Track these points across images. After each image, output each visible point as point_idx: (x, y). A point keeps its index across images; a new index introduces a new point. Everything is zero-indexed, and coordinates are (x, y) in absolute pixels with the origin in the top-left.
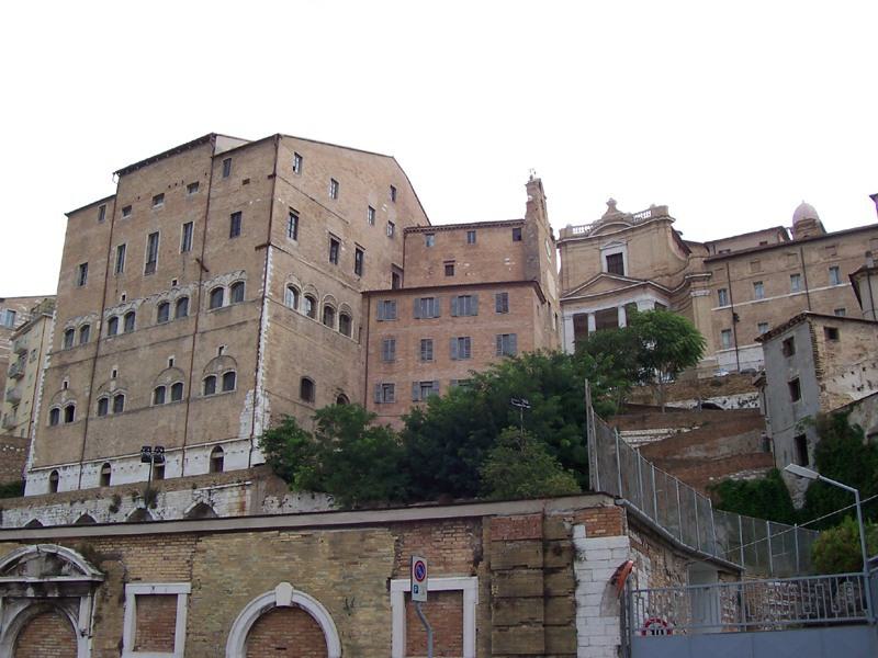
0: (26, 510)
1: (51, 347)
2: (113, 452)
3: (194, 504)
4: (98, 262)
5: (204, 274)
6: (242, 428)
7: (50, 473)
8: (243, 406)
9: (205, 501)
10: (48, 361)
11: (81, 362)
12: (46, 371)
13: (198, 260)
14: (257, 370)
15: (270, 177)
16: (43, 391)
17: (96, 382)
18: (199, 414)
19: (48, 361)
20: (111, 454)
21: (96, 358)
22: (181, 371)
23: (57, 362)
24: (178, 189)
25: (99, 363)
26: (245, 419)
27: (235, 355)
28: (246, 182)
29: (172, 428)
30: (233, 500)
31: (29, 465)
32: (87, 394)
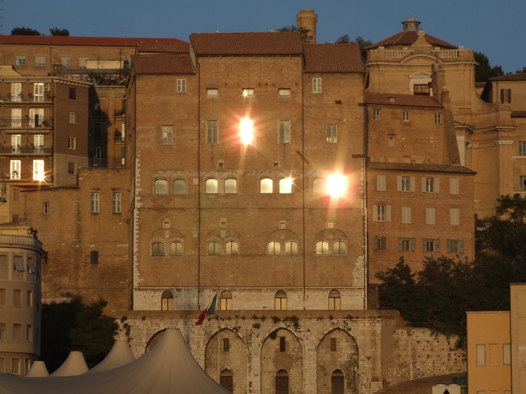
0: (158, 321)
1: (140, 190)
2: (232, 283)
3: (332, 329)
4: (186, 128)
5: (306, 164)
6: (355, 281)
7: (162, 292)
8: (354, 266)
9: (341, 327)
10: (139, 201)
11: (182, 209)
12: (139, 209)
13: (298, 153)
14: (364, 244)
15: (360, 104)
16: (139, 226)
17: (202, 228)
18: (315, 266)
19: (139, 201)
20: (230, 284)
21: (200, 209)
22: (294, 233)
23: (150, 204)
24: (269, 89)
25: (202, 213)
26: (355, 274)
27: (344, 230)
28: (338, 102)
29: (291, 274)
30: (366, 329)
31: (135, 284)
32: (195, 236)
